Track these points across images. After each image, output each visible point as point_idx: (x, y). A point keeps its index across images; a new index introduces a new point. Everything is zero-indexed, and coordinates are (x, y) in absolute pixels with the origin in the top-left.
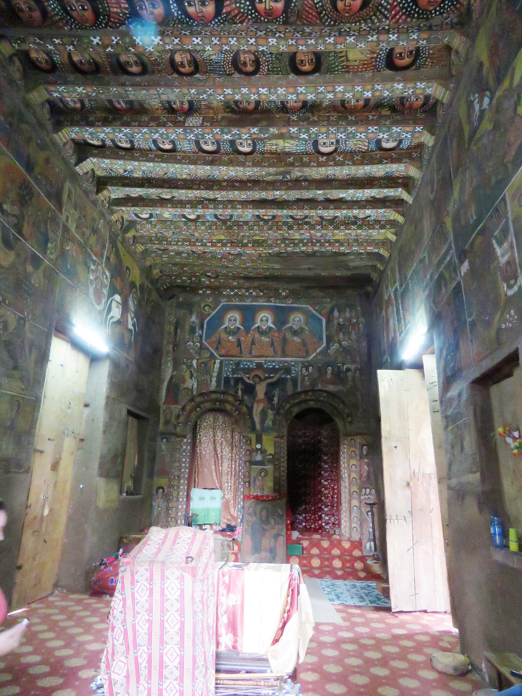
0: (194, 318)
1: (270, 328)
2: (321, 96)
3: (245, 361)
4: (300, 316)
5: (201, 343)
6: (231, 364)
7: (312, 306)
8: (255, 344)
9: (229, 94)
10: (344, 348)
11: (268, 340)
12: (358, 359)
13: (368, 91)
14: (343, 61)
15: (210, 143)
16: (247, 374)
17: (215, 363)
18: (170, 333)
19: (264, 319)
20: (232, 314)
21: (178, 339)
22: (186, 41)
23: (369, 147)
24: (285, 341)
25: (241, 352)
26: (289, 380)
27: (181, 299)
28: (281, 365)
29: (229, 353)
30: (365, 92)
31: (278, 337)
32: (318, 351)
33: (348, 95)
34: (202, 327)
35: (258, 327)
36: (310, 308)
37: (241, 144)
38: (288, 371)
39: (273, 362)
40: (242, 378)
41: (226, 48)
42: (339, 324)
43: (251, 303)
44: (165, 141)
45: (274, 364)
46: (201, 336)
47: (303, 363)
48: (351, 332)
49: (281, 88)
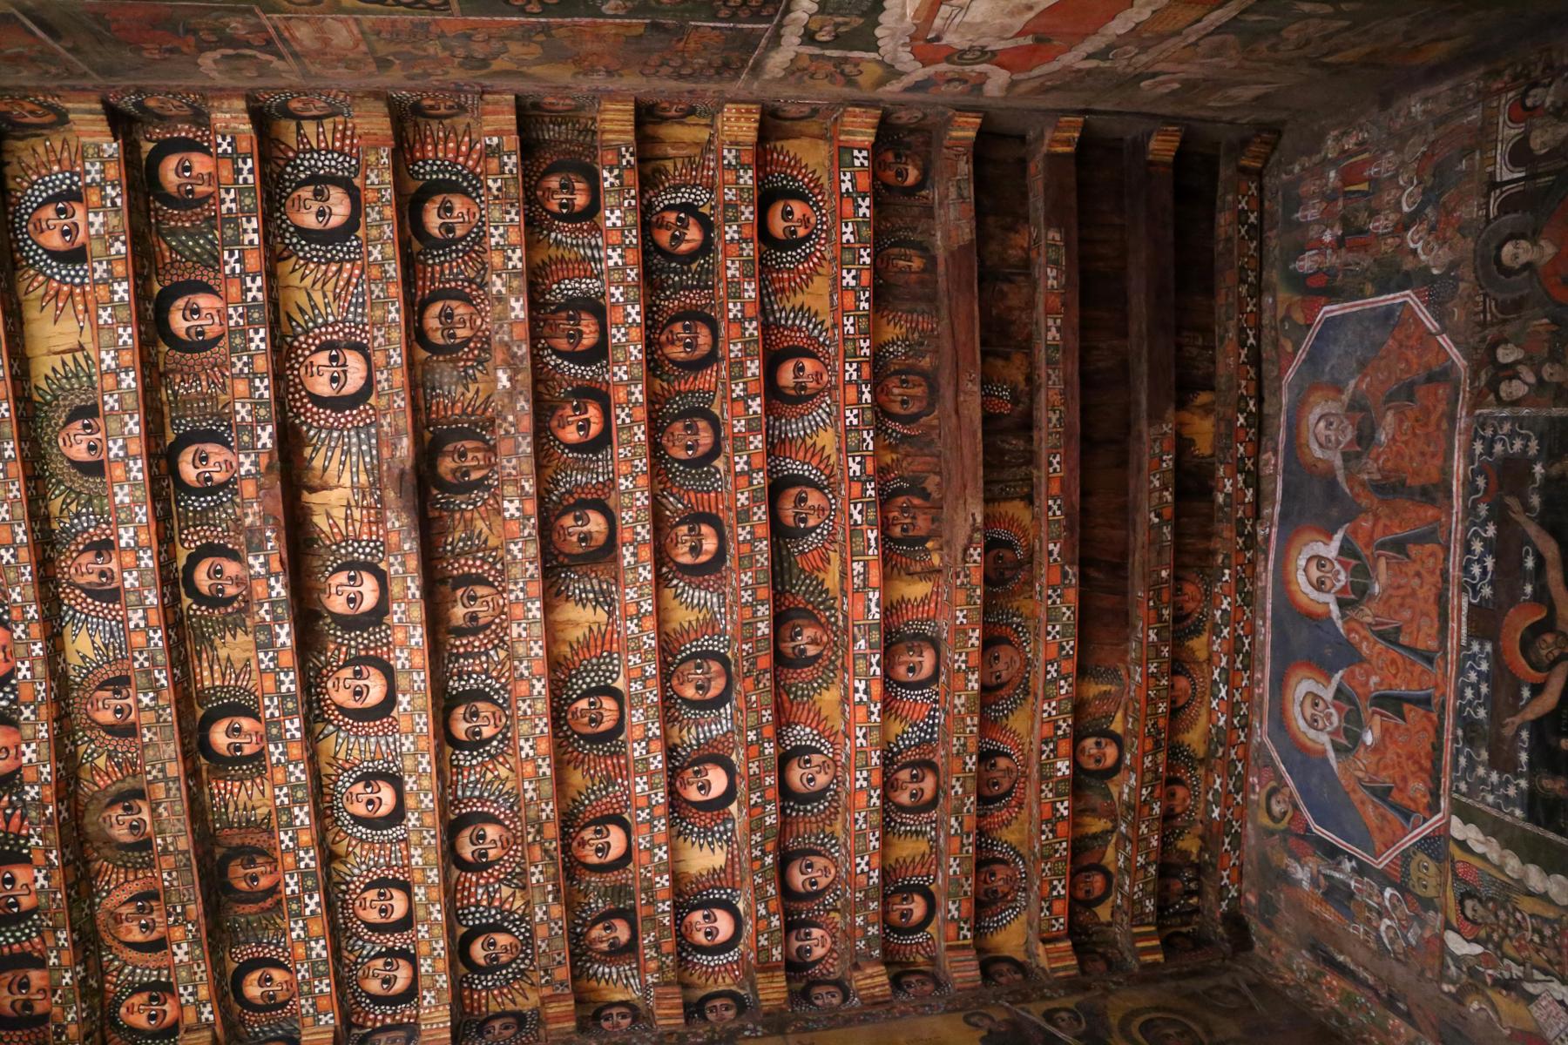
0: (1302, 874)
1: (1346, 550)
2: (130, 401)
3: (1460, 694)
4: (1313, 418)
5: (1384, 879)
6: (1472, 765)
7: (1282, 371)
8: (1398, 630)
9: (145, 618)
10: (1430, 196)
11: (1382, 563)
12: (1474, 116)
13: (114, 292)
14: (87, 358)
15: (361, 683)
16: (1519, 697)
17: (1463, 845)
18: (1348, 1000)
19: (1315, 573)
20: (1297, 709)
21: (1371, 981)
22: (25, 693)
23: (342, 261)
24: (1389, 488)
25: (1425, 702)
26: (1556, 470)
27: (1252, 899)
28: (1483, 509)
29: (1427, 764)
30: (116, 298)
31: (1377, 518)
32: (1431, 324)
33: (125, 337)
34: (1332, 852)
35: (1342, 604)
36: (1290, 374)
37: (350, 600)
38: (1510, 474)
39: (1468, 549)
40: (1537, 726)
41: (32, 612)
42: (1340, 243)
43: (1269, 623)
44: (364, 798)
45: (1478, 547)
46: (1362, 870)
47: (1477, 401)
48: (1370, 180)
49: (115, 494)
